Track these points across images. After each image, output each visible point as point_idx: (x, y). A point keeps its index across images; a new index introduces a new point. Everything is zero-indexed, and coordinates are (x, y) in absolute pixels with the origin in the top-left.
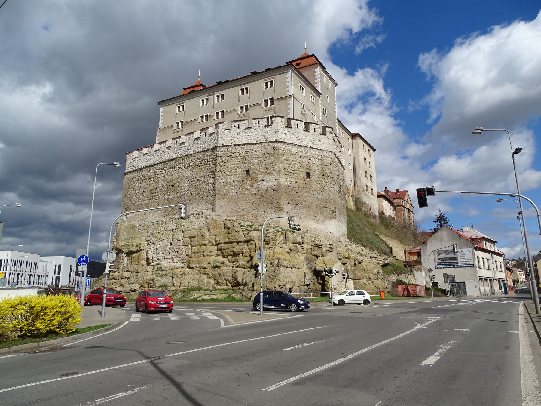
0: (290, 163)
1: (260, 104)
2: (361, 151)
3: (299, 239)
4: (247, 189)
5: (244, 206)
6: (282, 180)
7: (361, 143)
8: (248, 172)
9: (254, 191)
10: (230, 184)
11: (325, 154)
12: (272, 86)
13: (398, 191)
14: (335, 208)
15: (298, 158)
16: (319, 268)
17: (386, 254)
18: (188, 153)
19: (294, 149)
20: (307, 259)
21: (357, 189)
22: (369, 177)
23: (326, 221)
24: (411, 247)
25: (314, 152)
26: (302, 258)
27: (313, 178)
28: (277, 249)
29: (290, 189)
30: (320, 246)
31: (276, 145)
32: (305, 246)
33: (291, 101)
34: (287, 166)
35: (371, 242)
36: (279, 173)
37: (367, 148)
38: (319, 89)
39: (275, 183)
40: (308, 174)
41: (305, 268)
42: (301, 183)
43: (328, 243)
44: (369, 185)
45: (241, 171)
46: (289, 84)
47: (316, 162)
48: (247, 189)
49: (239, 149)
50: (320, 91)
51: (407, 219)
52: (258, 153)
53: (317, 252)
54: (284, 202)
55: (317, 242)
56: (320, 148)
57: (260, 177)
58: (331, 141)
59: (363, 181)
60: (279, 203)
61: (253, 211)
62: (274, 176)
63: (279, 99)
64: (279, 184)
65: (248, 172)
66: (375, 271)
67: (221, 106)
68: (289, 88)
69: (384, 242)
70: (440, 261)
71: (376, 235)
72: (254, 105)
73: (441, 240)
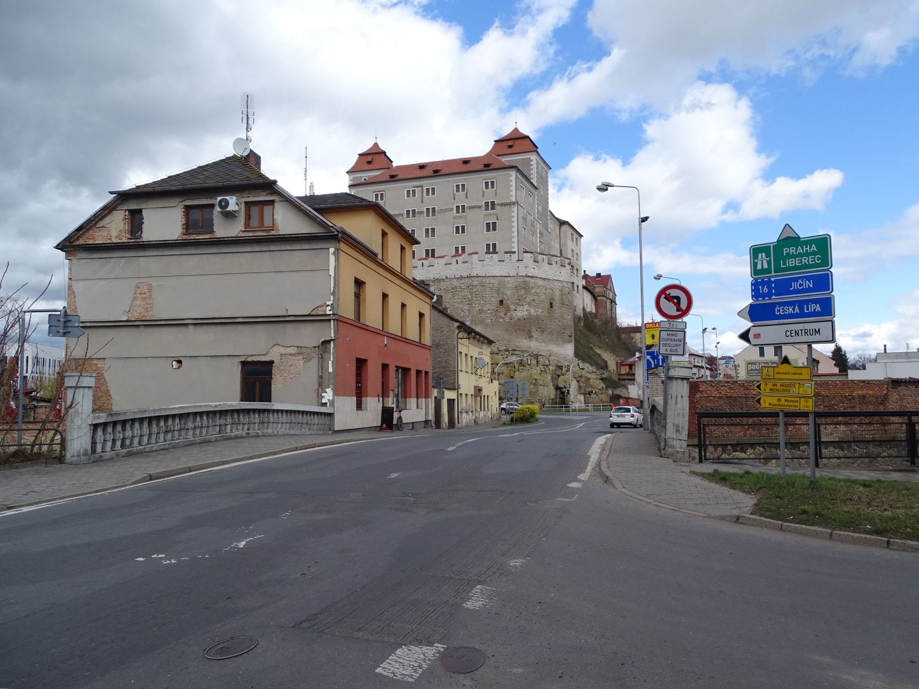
0: (538, 295)
1: (480, 207)
2: (569, 242)
3: (547, 362)
4: (501, 317)
5: (499, 332)
6: (532, 311)
7: (570, 231)
8: (501, 302)
9: (507, 319)
10: (486, 312)
12: (493, 187)
13: (599, 275)
16: (561, 385)
17: (602, 368)
18: (437, 276)
19: (541, 283)
20: (552, 378)
22: (575, 272)
24: (623, 359)
25: (555, 283)
26: (549, 377)
27: (555, 308)
28: (534, 371)
29: (537, 318)
30: (560, 368)
31: (527, 279)
32: (551, 367)
33: (515, 209)
34: (536, 298)
35: (589, 357)
36: (530, 305)
37: (575, 235)
38: (534, 181)
39: (526, 313)
41: (551, 386)
42: (546, 312)
43: (567, 364)
44: (575, 281)
45: (495, 300)
46: (513, 188)
47: (557, 293)
48: (501, 317)
49: (493, 281)
50: (536, 184)
51: (609, 312)
52: (510, 285)
53: (559, 372)
54: (533, 330)
57: (513, 307)
58: (569, 272)
60: (530, 332)
61: (506, 336)
62: (526, 307)
64: (530, 314)
65: (501, 302)
66: (600, 387)
67: (430, 201)
69: (599, 355)
71: (591, 348)
72: (473, 207)
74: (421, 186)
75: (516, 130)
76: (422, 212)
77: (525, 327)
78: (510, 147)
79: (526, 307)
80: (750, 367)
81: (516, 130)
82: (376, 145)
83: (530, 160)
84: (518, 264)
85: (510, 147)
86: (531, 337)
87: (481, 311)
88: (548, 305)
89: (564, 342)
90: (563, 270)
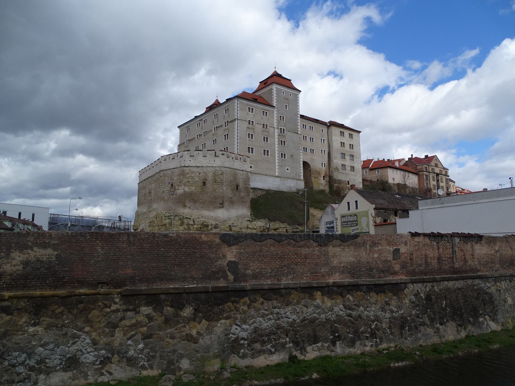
0: (193, 178)
1: (222, 126)
11: (217, 169)
14: (223, 202)
15: (198, 175)
19: (196, 170)
21: (331, 170)
23: (216, 210)
25: (209, 169)
29: (191, 194)
30: (207, 226)
36: (185, 185)
39: (183, 191)
40: (204, 183)
43: (214, 223)
46: (236, 110)
49: (169, 172)
52: (176, 174)
55: (205, 224)
56: (214, 165)
59: (337, 161)
60: (184, 203)
62: (183, 187)
63: (231, 122)
64: (185, 191)
68: (236, 114)
70: (327, 229)
73: (328, 214)
74: (202, 120)
75: (275, 72)
76: (201, 135)
77: (183, 200)
78: (265, 84)
79: (183, 187)
80: (345, 219)
81: (275, 72)
82: (217, 100)
83: (272, 89)
84: (181, 159)
85: (265, 84)
86: (185, 206)
87: (163, 192)
88: (202, 184)
89: (216, 208)
90: (217, 159)
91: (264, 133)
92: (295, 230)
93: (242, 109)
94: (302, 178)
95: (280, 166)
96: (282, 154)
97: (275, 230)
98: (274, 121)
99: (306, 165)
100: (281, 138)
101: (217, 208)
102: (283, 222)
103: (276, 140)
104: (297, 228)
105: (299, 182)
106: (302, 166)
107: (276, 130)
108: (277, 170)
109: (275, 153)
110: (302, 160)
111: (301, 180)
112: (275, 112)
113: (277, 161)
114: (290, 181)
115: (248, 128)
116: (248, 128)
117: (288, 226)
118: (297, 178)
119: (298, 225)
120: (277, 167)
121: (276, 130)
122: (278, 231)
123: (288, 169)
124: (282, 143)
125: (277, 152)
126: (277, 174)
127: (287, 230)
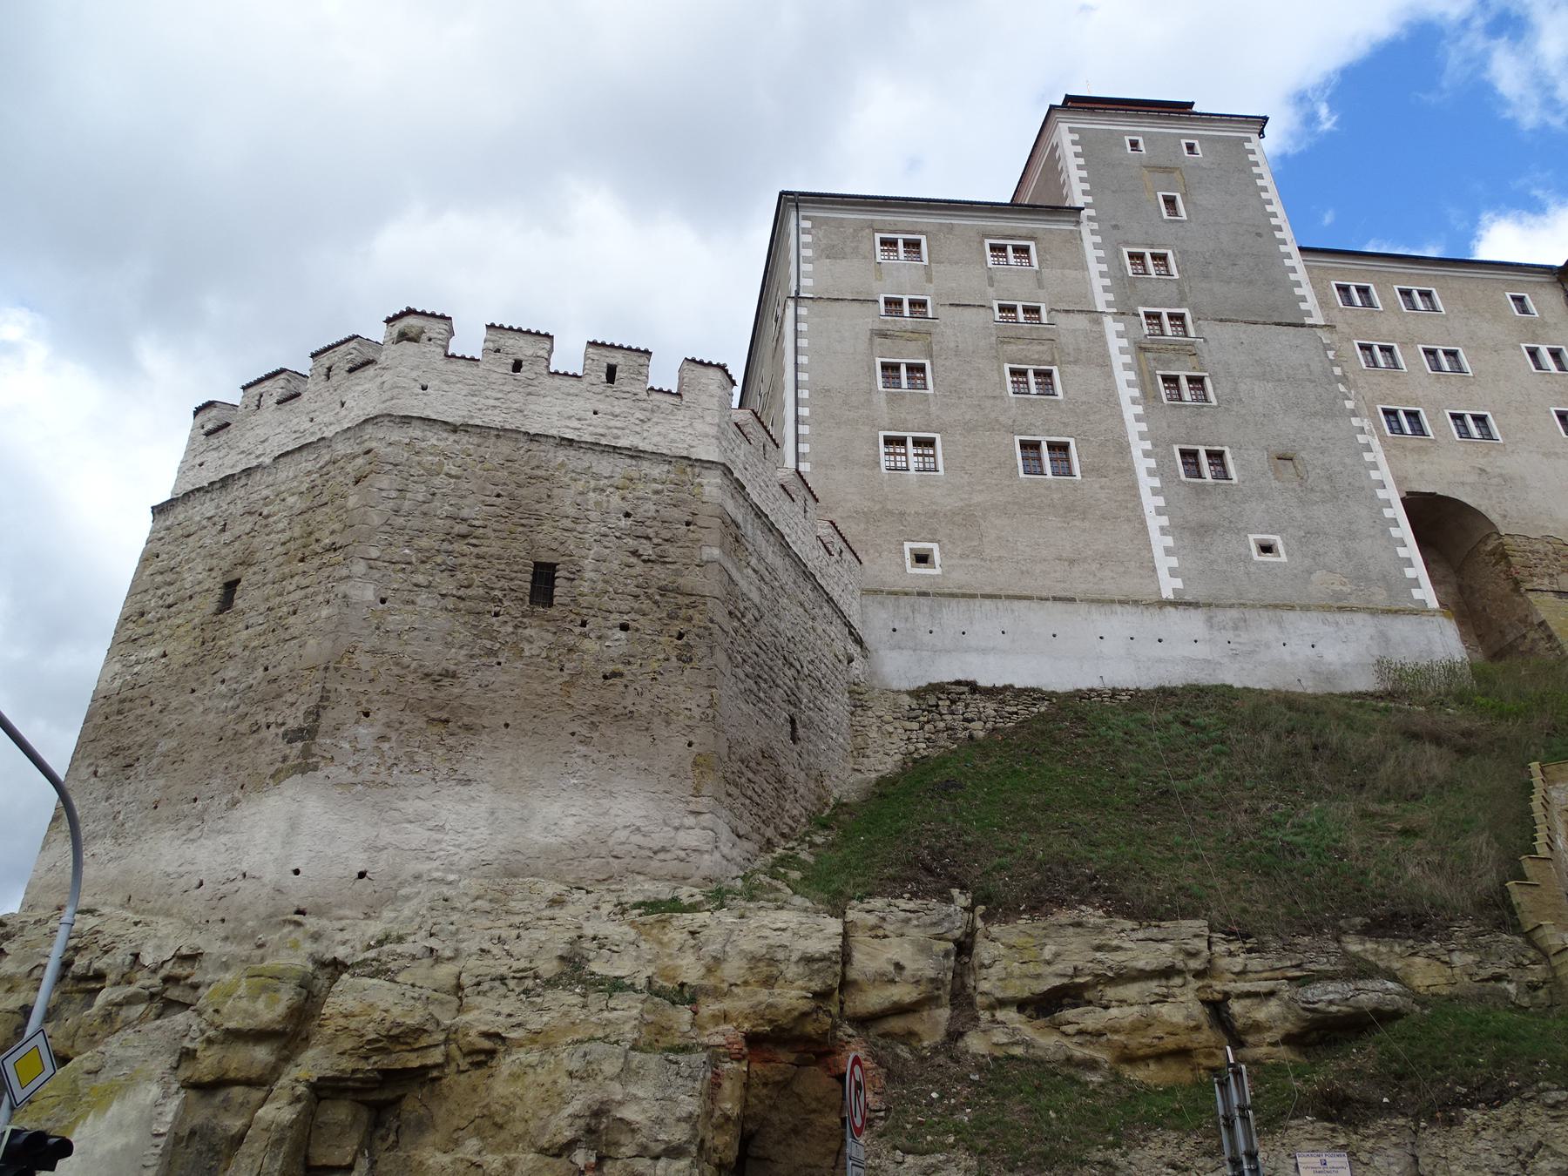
91: (1011, 349)
92: (1329, 996)
93: (830, 252)
94: (1426, 593)
95: (1193, 533)
96: (1189, 456)
97: (1045, 1006)
98: (1087, 282)
99: (1439, 522)
100: (1167, 364)
101: (260, 788)
102: (1147, 914)
103: (1123, 377)
104: (1361, 970)
105: (1401, 628)
106: (1405, 530)
107: (1111, 326)
108: (1164, 564)
109: (1124, 449)
110: (1393, 495)
111: (1420, 610)
112: (1089, 240)
113: (1150, 502)
114: (1304, 626)
115: (884, 335)
116: (884, 335)
117: (1231, 959)
118: (1380, 598)
119: (1377, 928)
120: (1160, 542)
121: (1111, 326)
122: (1091, 1018)
123: (1266, 549)
124: (1175, 385)
125: (1138, 447)
126: (1169, 587)
127: (1217, 1008)
